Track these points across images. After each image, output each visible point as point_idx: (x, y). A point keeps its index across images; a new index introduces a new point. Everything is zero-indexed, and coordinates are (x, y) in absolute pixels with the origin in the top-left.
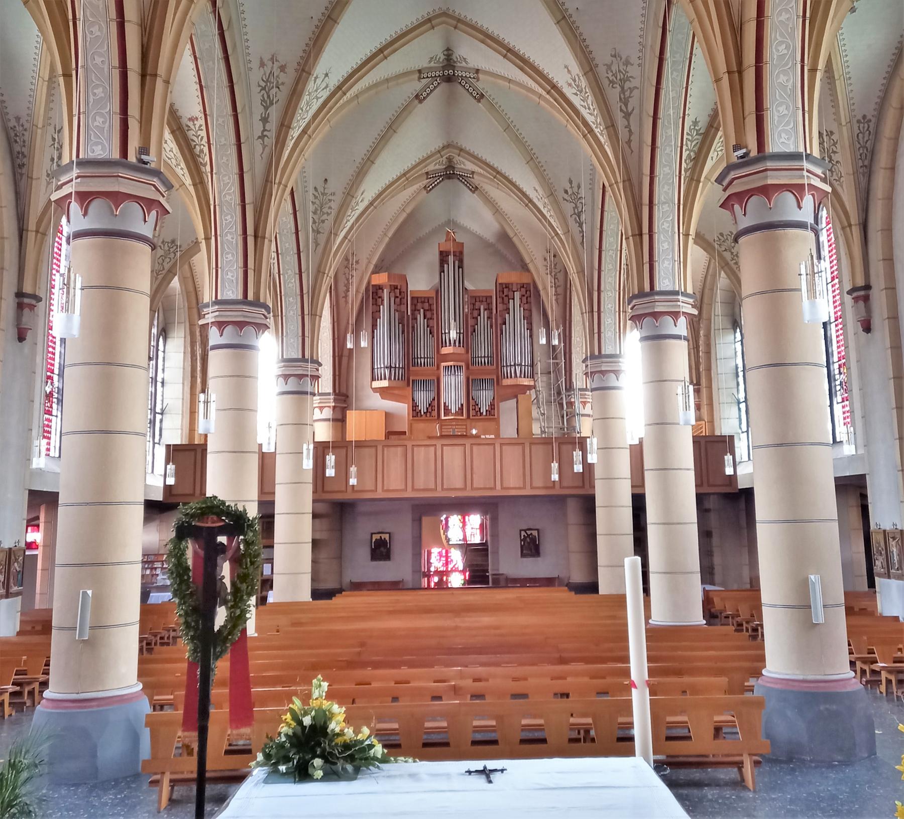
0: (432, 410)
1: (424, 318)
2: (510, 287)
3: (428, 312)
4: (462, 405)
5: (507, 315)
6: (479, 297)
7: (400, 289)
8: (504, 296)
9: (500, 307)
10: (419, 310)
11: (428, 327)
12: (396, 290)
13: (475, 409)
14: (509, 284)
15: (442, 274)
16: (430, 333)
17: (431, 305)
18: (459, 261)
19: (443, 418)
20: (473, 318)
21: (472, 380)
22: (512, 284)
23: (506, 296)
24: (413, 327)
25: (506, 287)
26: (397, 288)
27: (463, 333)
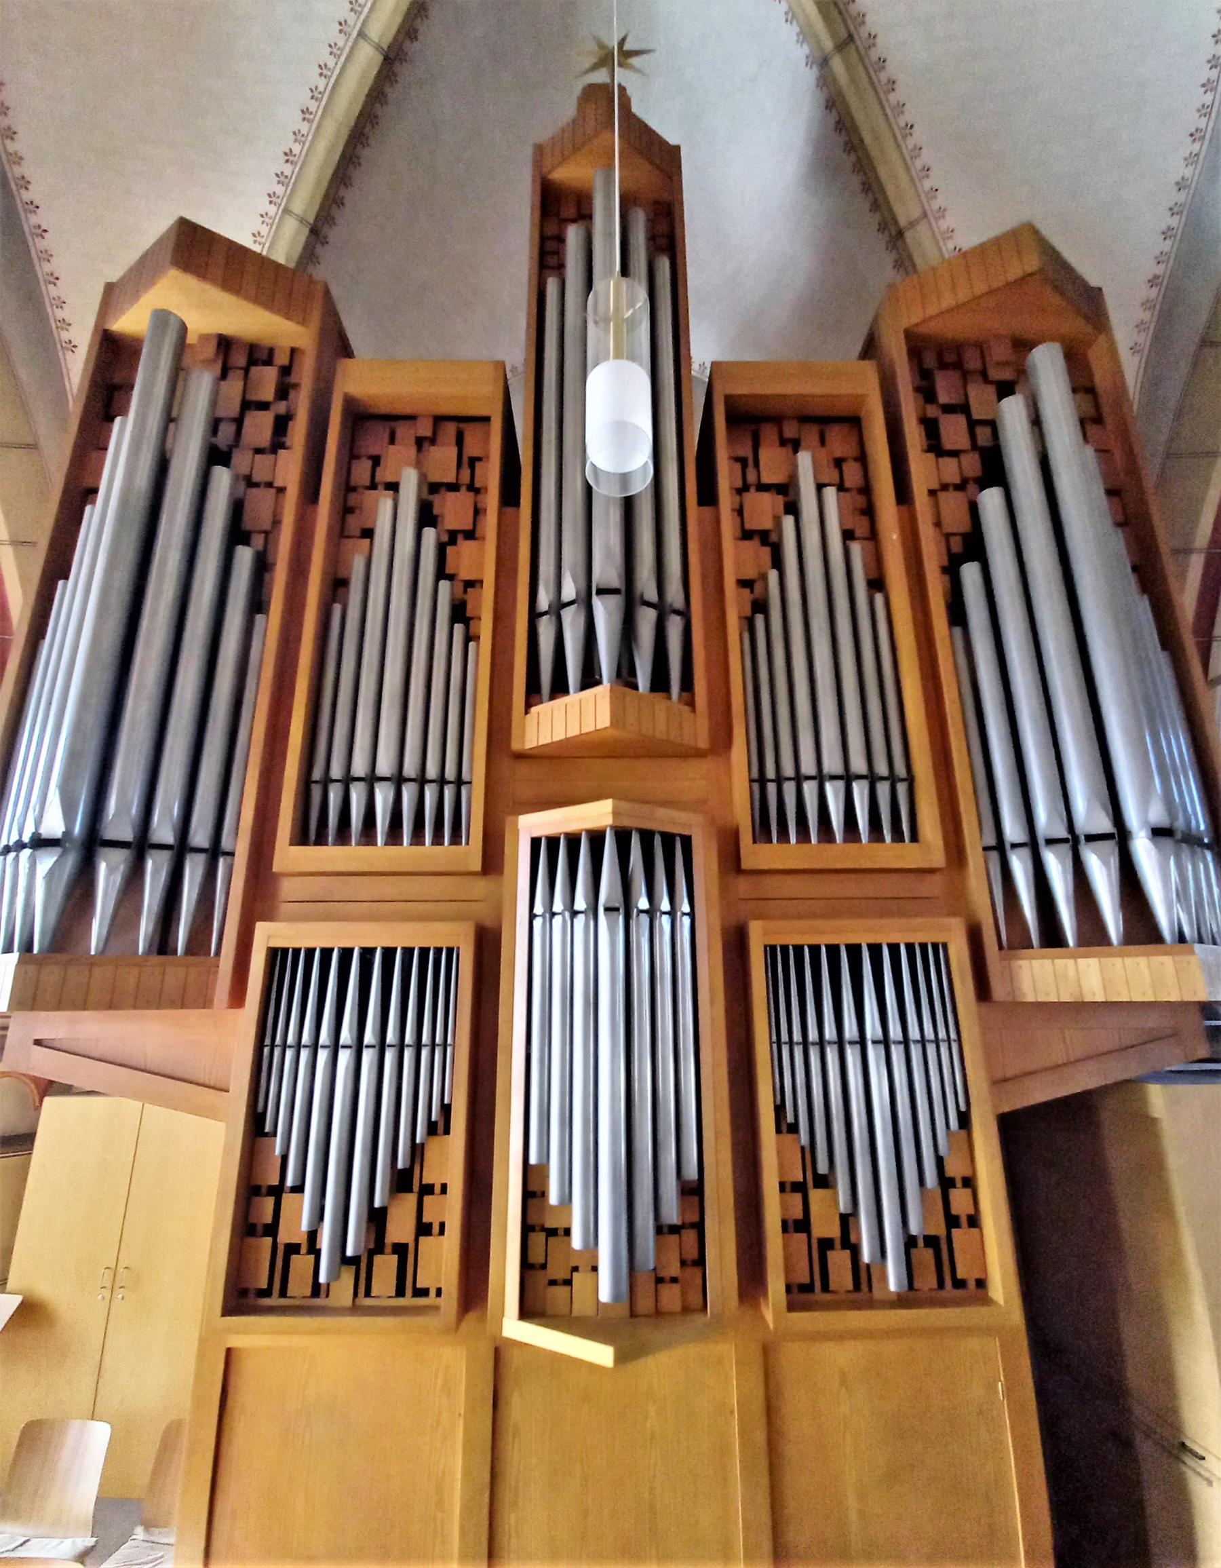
0: (423, 1229)
1: (426, 516)
2: (972, 362)
3: (451, 496)
4: (693, 1191)
5: (991, 500)
6: (777, 420)
7: (286, 371)
8: (932, 411)
9: (922, 470)
10: (394, 487)
11: (441, 573)
12: (255, 371)
13: (803, 1225)
14: (958, 347)
15: (552, 285)
16: (459, 613)
17: (473, 461)
18: (651, 222)
19: (514, 1328)
20: (747, 535)
21: (770, 951)
22: (980, 347)
23: (948, 409)
24: (337, 585)
25: (943, 366)
26: (268, 362)
27: (685, 614)
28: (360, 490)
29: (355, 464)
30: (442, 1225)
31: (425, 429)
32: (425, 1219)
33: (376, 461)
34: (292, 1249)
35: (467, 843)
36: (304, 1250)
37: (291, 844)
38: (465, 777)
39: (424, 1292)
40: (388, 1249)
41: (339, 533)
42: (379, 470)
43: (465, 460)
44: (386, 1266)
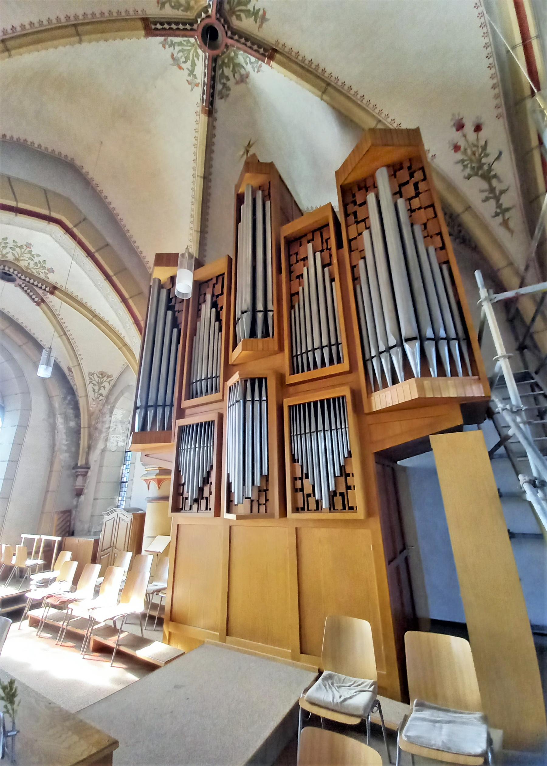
28: (294, 265)
29: (291, 257)
30: (354, 486)
31: (310, 237)
32: (348, 485)
33: (297, 254)
34: (309, 495)
35: (344, 362)
36: (312, 495)
37: (290, 375)
38: (339, 342)
39: (351, 508)
40: (338, 495)
41: (290, 280)
42: (298, 256)
43: (324, 241)
44: (338, 500)
